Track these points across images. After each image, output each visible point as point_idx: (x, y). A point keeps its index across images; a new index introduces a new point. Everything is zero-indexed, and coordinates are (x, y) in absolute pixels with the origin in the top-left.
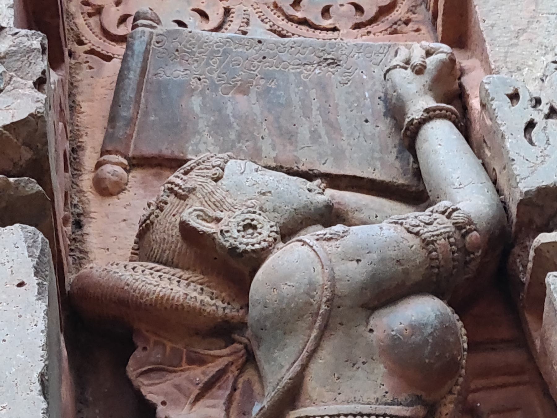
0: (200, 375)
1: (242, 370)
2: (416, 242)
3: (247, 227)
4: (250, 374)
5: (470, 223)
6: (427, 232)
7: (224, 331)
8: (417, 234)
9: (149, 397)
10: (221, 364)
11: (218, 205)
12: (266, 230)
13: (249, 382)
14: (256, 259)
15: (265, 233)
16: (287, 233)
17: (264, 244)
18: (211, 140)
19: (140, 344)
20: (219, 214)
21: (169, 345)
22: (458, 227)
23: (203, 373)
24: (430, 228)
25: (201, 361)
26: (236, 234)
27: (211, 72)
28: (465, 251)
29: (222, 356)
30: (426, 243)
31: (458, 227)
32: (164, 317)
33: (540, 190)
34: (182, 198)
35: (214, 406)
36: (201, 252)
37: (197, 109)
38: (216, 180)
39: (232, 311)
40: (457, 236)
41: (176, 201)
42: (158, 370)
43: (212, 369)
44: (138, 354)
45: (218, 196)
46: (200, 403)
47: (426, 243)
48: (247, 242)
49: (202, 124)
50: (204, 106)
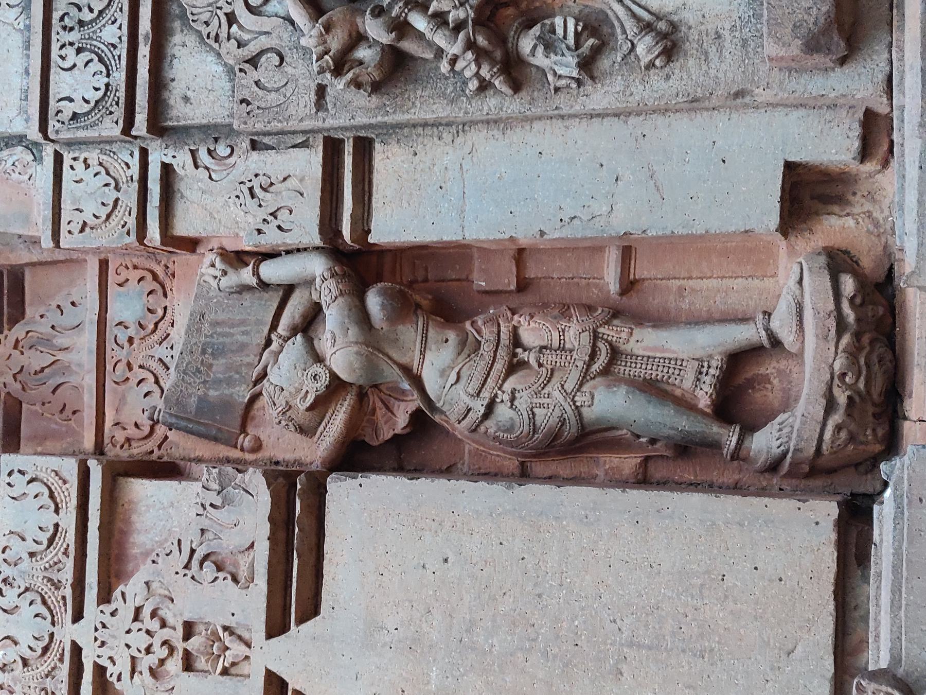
0: (381, 412)
1: (381, 391)
2: (340, 299)
3: (315, 379)
4: (383, 388)
5: (330, 269)
6: (335, 292)
7: (362, 395)
8: (336, 298)
9: (389, 437)
10: (377, 400)
11: (299, 390)
12: (317, 369)
13: (388, 389)
14: (334, 376)
15: (320, 370)
16: (319, 359)
17: (327, 372)
18: (237, 388)
19: (363, 438)
20: (304, 391)
21: (364, 424)
22: (332, 276)
23: (380, 409)
24: (333, 290)
25: (374, 410)
26: (319, 384)
27: (195, 382)
28: (344, 275)
29: (374, 399)
30: (341, 294)
31: (332, 276)
32: (352, 425)
33: (320, 233)
34: (290, 407)
35: (399, 407)
36: (321, 404)
37: (216, 393)
38: (283, 390)
39: (354, 391)
40: (337, 277)
41: (291, 411)
42: (376, 431)
43: (379, 404)
44: (367, 440)
45: (293, 390)
46: (395, 412)
47: (341, 294)
48: (324, 380)
49: (226, 392)
50: (216, 390)
